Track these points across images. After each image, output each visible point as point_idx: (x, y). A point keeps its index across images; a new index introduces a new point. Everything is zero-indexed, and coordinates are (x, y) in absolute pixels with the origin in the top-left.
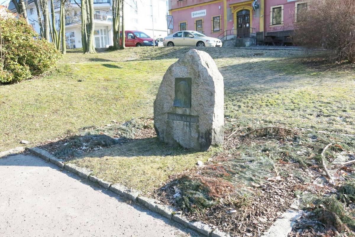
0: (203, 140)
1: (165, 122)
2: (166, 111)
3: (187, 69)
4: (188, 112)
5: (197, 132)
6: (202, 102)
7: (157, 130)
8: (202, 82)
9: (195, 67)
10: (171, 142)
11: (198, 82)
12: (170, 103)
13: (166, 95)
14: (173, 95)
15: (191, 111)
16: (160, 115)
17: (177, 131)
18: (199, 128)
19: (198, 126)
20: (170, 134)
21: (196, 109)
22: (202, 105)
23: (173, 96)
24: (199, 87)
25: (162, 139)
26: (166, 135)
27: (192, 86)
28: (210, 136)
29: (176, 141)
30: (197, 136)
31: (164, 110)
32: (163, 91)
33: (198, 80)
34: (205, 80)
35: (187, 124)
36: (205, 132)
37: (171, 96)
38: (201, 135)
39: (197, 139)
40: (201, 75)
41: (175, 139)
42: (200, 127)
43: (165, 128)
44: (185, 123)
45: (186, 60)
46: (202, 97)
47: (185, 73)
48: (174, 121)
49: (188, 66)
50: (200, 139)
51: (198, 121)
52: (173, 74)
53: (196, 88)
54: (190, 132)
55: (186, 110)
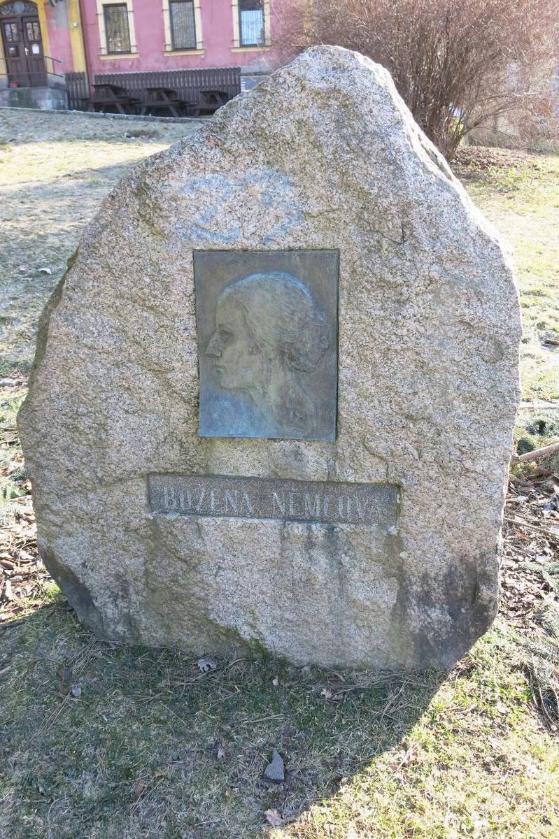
0: (435, 614)
1: (127, 530)
2: (129, 466)
3: (297, 190)
4: (314, 462)
5: (388, 575)
6: (425, 400)
7: (76, 579)
8: (435, 275)
9: (366, 173)
10: (195, 641)
11: (399, 280)
12: (152, 411)
13: (117, 365)
14: (177, 365)
15: (336, 456)
16: (82, 490)
17: (233, 576)
18: (403, 555)
19: (394, 544)
20: (177, 598)
21: (381, 447)
22: (428, 419)
23: (184, 371)
24: (408, 311)
25: (120, 628)
26: (145, 605)
27: (342, 301)
28: (483, 588)
29: (232, 633)
30: (390, 599)
31: (114, 456)
32: (89, 341)
33: (395, 261)
34: (448, 266)
35: (309, 537)
36: (445, 570)
37: (159, 371)
38: (416, 588)
39: (393, 615)
40: (421, 231)
41: (222, 624)
42: (411, 544)
43: (134, 564)
44: (298, 529)
45: (285, 127)
46: (433, 371)
47: (277, 218)
48: (204, 521)
49: (303, 170)
50: (414, 611)
51: (398, 511)
52: (171, 224)
53: (382, 320)
54: (342, 578)
55: (297, 454)
